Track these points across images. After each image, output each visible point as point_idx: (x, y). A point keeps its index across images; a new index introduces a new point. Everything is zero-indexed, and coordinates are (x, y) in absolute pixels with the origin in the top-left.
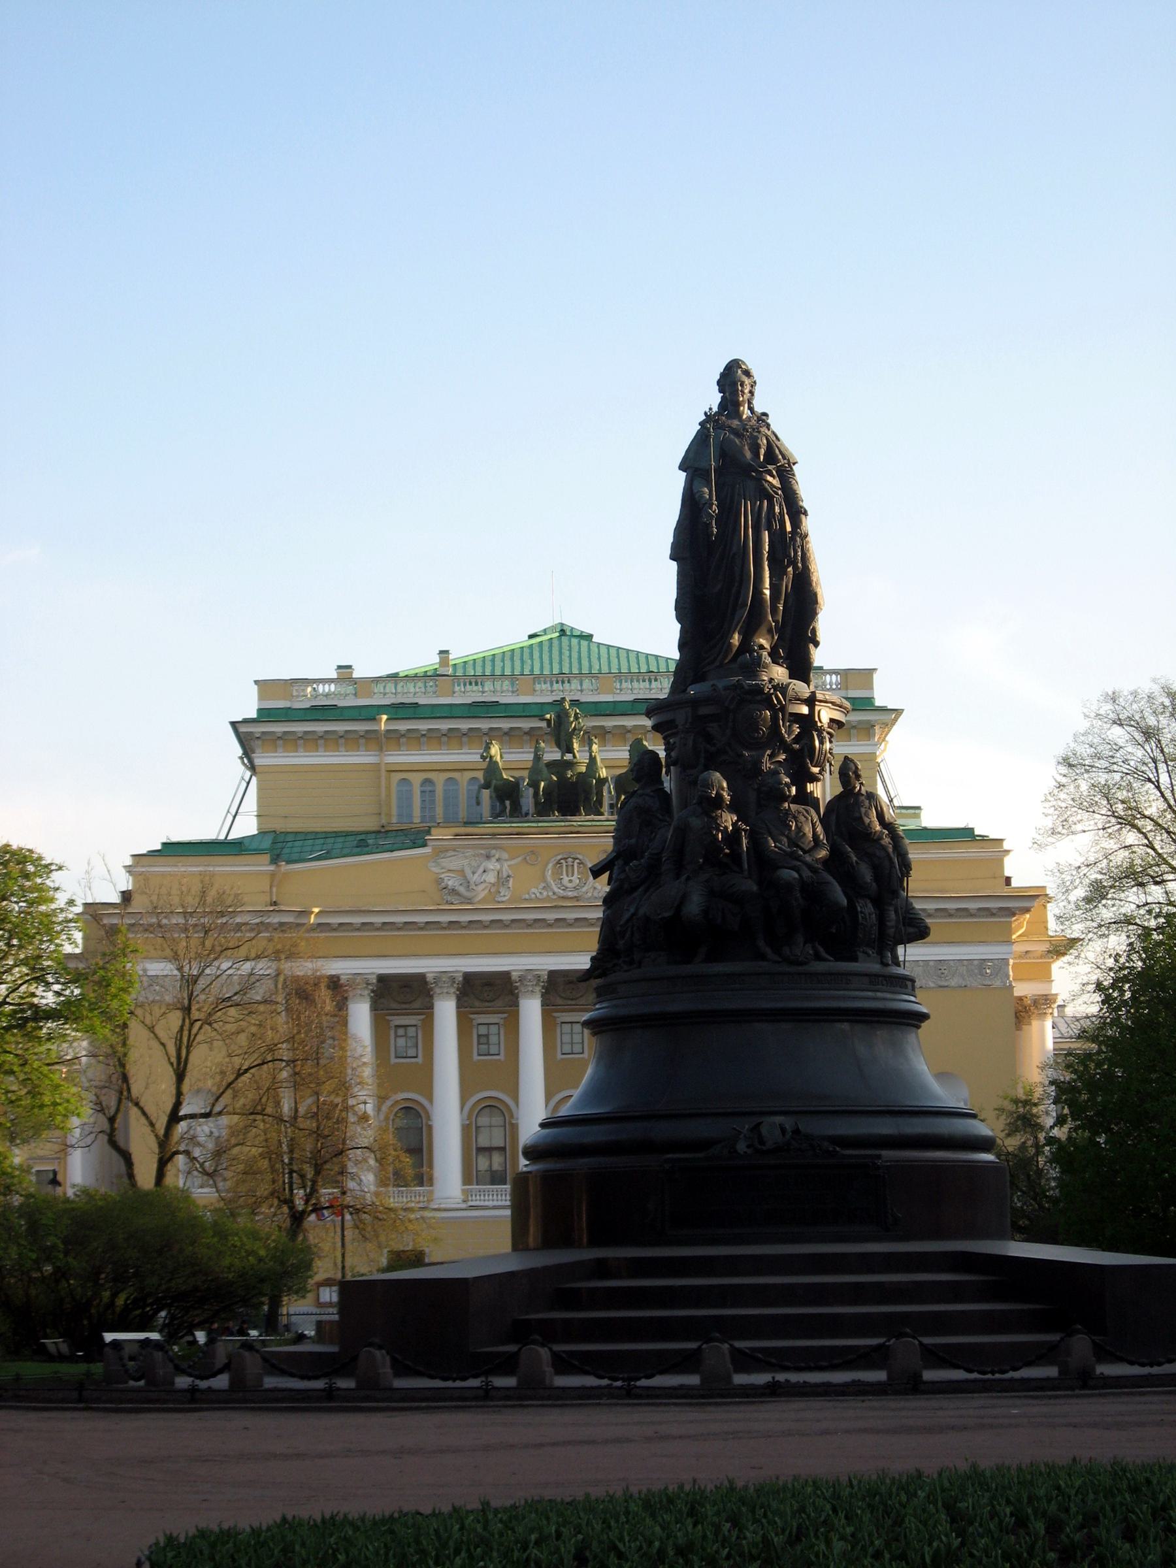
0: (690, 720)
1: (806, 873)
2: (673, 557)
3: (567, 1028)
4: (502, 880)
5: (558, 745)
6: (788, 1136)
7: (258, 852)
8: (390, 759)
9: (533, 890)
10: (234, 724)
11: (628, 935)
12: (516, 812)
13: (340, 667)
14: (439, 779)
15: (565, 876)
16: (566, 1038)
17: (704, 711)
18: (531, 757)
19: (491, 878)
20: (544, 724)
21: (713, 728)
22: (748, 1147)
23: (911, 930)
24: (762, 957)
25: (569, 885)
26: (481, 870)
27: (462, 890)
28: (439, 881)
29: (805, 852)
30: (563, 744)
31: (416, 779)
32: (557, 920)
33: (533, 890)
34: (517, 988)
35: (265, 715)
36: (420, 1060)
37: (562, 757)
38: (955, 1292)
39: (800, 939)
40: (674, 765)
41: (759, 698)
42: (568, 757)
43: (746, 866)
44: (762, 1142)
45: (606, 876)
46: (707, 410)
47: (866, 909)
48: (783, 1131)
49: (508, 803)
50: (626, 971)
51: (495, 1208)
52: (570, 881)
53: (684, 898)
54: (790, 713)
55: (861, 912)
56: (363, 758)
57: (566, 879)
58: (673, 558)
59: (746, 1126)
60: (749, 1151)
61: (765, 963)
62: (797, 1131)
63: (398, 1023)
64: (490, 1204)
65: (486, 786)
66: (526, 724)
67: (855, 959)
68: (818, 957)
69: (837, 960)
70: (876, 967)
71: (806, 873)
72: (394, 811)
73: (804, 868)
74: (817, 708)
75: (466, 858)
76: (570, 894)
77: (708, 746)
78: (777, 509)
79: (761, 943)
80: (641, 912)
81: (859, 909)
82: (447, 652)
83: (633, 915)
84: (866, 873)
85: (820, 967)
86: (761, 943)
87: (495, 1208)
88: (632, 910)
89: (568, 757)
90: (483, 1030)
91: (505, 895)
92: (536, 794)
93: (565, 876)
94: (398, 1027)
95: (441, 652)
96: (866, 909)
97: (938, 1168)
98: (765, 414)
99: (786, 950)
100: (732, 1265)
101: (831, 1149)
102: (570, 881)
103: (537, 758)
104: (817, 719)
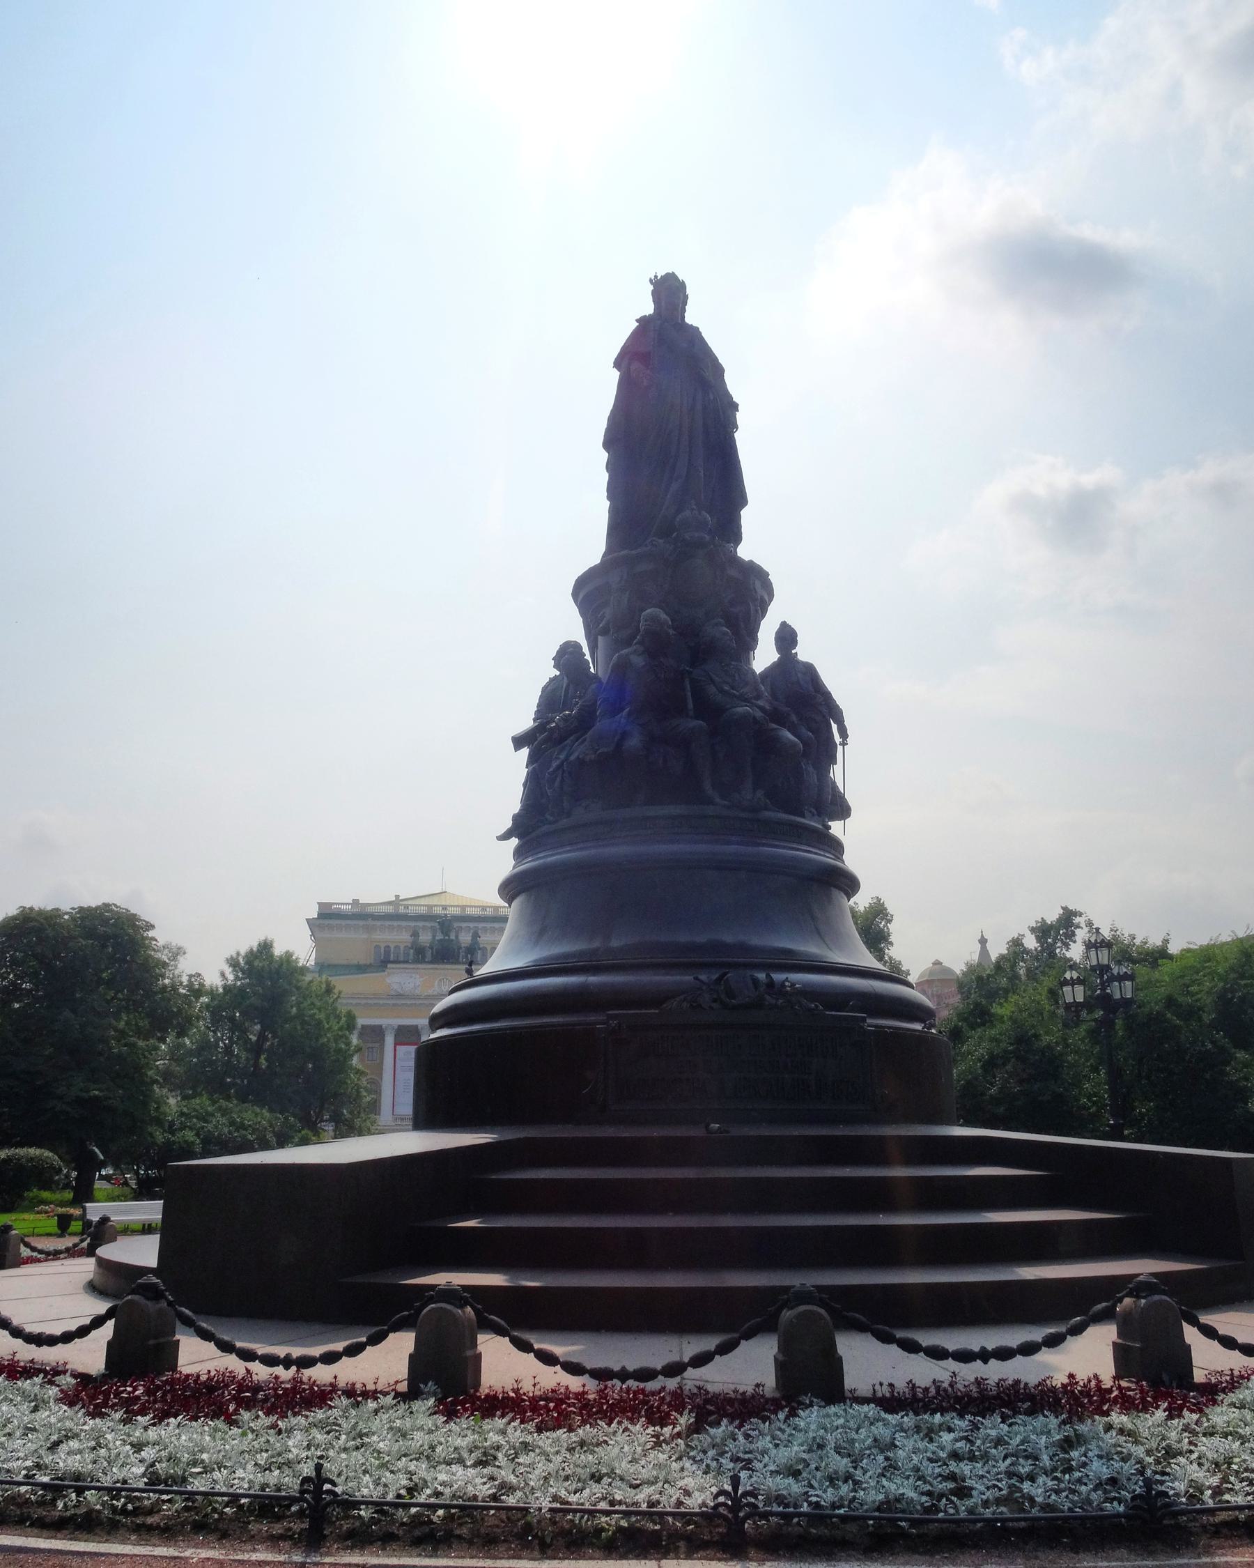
2: (608, 444)
5: (442, 933)
11: (557, 784)
12: (422, 961)
14: (392, 946)
18: (431, 937)
20: (436, 924)
35: (322, 915)
40: (605, 632)
42: (447, 938)
43: (690, 705)
45: (525, 752)
48: (756, 982)
50: (550, 823)
53: (624, 735)
57: (443, 988)
62: (771, 984)
65: (412, 948)
66: (428, 924)
68: (766, 809)
80: (572, 758)
83: (562, 764)
86: (708, 786)
88: (562, 757)
89: (447, 938)
92: (432, 953)
103: (434, 937)
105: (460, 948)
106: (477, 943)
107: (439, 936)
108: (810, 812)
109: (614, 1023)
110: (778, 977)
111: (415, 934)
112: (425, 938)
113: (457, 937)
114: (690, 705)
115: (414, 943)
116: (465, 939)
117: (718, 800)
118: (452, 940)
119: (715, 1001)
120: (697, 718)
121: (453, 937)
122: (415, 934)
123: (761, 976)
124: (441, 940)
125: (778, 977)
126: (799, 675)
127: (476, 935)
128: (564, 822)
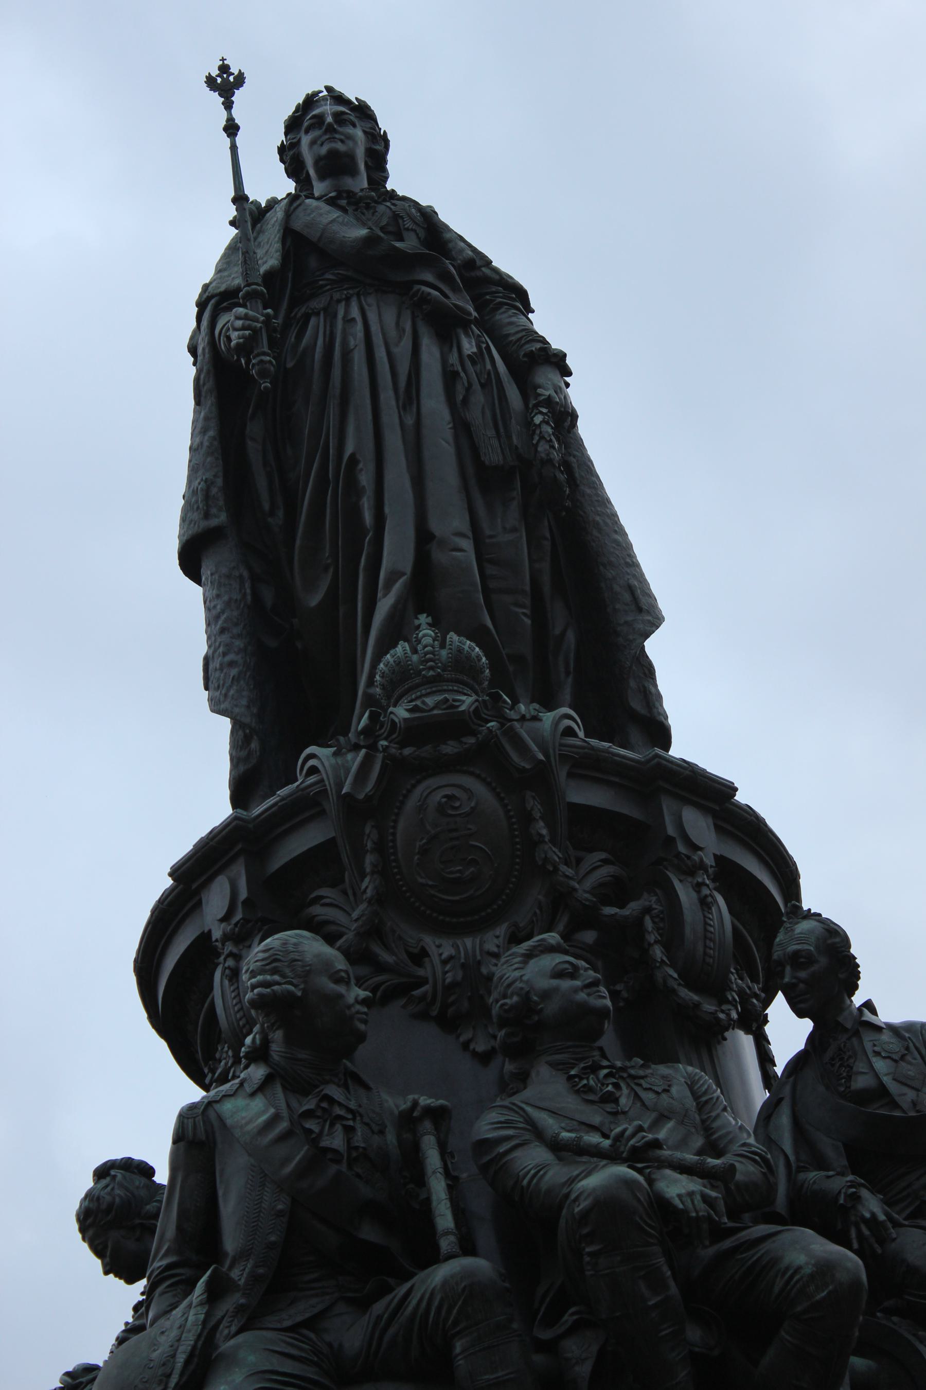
0: (243, 894)
41: (450, 748)
43: (445, 1219)
46: (215, 72)
54: (573, 807)
74: (668, 806)
114: (445, 1219)
120: (468, 1248)
126: (880, 1065)
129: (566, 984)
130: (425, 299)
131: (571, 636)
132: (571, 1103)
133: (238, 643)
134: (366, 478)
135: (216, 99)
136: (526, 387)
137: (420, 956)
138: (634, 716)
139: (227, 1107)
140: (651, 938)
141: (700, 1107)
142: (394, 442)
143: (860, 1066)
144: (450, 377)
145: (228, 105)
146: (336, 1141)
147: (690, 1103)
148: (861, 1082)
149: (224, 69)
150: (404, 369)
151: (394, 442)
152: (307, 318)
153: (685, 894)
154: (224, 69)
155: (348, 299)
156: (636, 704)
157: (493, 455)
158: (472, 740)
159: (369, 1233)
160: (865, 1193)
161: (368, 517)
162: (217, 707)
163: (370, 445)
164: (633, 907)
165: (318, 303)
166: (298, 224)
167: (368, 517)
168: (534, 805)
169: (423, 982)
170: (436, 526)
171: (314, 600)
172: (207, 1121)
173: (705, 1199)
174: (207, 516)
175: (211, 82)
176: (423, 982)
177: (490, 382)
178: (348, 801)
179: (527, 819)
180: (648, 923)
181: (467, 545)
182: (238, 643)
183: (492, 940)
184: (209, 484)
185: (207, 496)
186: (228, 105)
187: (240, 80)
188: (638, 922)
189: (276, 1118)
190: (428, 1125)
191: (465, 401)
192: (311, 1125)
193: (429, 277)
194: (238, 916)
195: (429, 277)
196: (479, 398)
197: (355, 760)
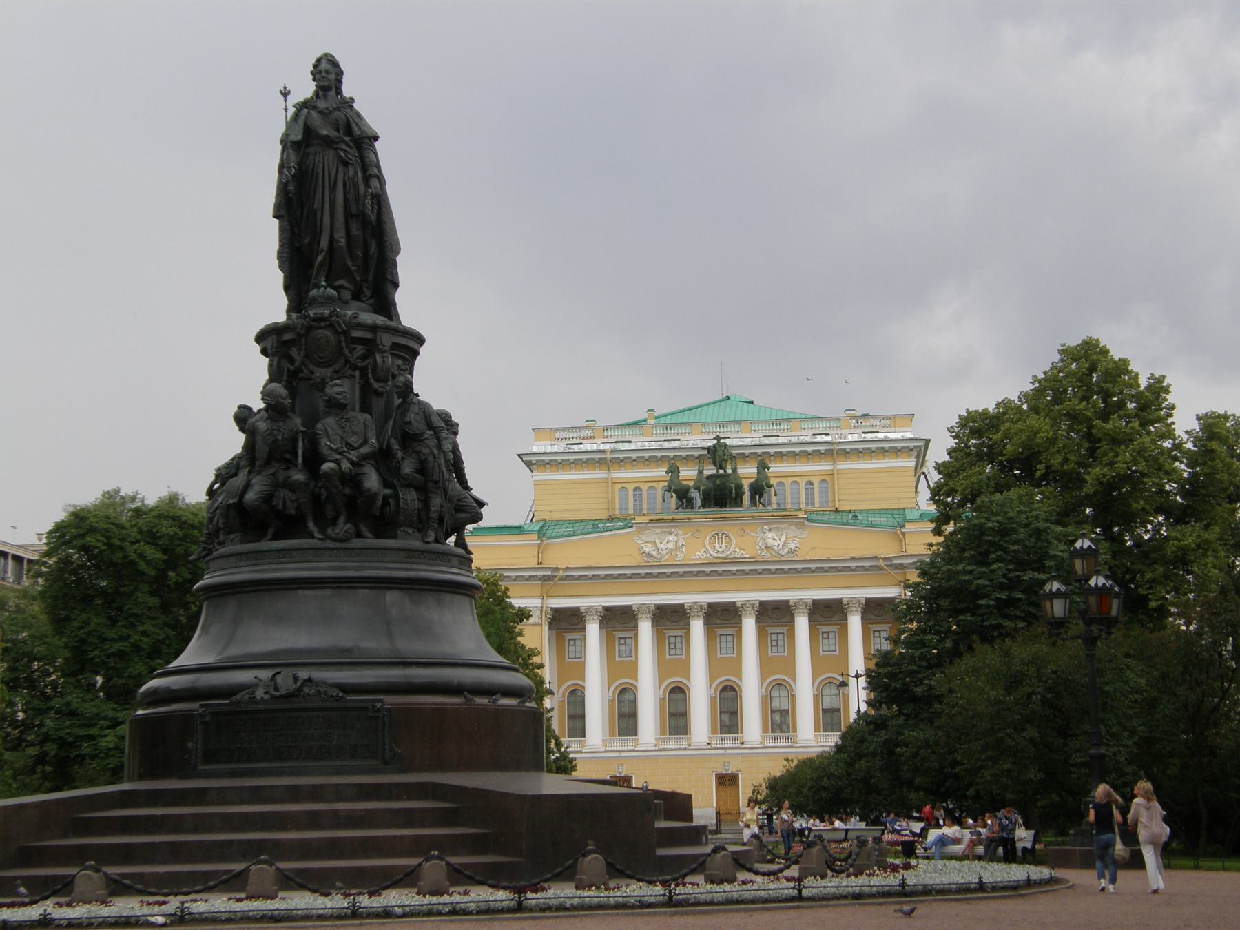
1: (346, 465)
3: (723, 638)
4: (678, 548)
6: (298, 684)
7: (532, 532)
8: (614, 476)
9: (697, 553)
10: (519, 455)
12: (690, 504)
13: (587, 421)
14: (645, 487)
15: (717, 544)
16: (724, 645)
17: (287, 337)
19: (671, 546)
21: (294, 352)
22: (266, 693)
23: (463, 515)
24: (313, 537)
25: (720, 550)
26: (666, 541)
27: (654, 553)
28: (640, 549)
29: (354, 448)
30: (718, 464)
31: (631, 487)
32: (712, 572)
33: (697, 553)
34: (688, 613)
36: (633, 658)
37: (718, 471)
38: (408, 818)
39: (342, 520)
41: (323, 324)
42: (721, 471)
44: (276, 689)
46: (282, 89)
47: (410, 498)
48: (296, 678)
49: (685, 501)
51: (680, 749)
52: (721, 547)
53: (247, 486)
55: (403, 498)
56: (599, 475)
58: (276, 217)
59: (264, 674)
60: (266, 697)
61: (310, 541)
63: (620, 636)
64: (673, 747)
67: (394, 537)
68: (359, 535)
69: (378, 536)
70: (416, 544)
71: (346, 465)
72: (617, 506)
73: (345, 461)
74: (379, 334)
75: (657, 534)
76: (720, 555)
77: (289, 366)
78: (351, 172)
79: (311, 525)
81: (401, 495)
82: (653, 410)
84: (408, 468)
85: (357, 543)
86: (311, 525)
87: (680, 749)
89: (721, 471)
90: (672, 640)
91: (680, 558)
93: (717, 544)
94: (620, 638)
95: (649, 410)
96: (410, 498)
97: (440, 711)
98: (352, 99)
99: (329, 531)
100: (256, 795)
101: (335, 694)
102: (721, 547)
103: (701, 472)
104: (378, 342)
105: (739, 487)
106: (767, 478)
107: (710, 470)
108: (406, 532)
109: (201, 711)
110: (318, 674)
111: (673, 471)
112: (688, 474)
113: (734, 470)
115: (670, 483)
116: (747, 472)
117: (316, 534)
118: (729, 475)
119: (266, 693)
121: (729, 471)
122: (673, 471)
123: (303, 674)
124: (709, 477)
125: (318, 674)
126: (412, 415)
127: (763, 467)
128: (222, 551)
129: (339, 397)
130: (340, 156)
131: (375, 256)
132: (335, 426)
133: (286, 250)
134: (319, 216)
135: (282, 97)
136: (368, 185)
137: (312, 373)
138: (388, 280)
139: (258, 423)
140: (370, 371)
141: (365, 428)
142: (327, 206)
143: (408, 415)
144: (345, 185)
145: (285, 101)
146: (280, 437)
147: (363, 428)
148: (407, 419)
149: (285, 88)
150: (333, 179)
151: (327, 206)
152: (309, 154)
153: (378, 359)
154: (285, 88)
155: (320, 152)
156: (389, 277)
157: (354, 210)
158: (327, 323)
159: (287, 456)
160: (399, 452)
161: (318, 229)
162: (281, 267)
163: (320, 206)
164: (367, 362)
165: (312, 150)
166: (308, 123)
167: (318, 229)
168: (343, 338)
169: (312, 379)
170: (336, 236)
171: (306, 241)
172: (254, 427)
173: (350, 470)
174: (280, 211)
175: (281, 92)
176: (312, 379)
177: (356, 186)
178: (299, 335)
179: (340, 342)
180: (369, 367)
181: (343, 241)
182: (286, 250)
183: (328, 372)
184: (281, 202)
185: (279, 205)
186: (285, 101)
187: (289, 93)
188: (365, 368)
189: (267, 430)
190: (300, 434)
191: (349, 193)
192: (275, 432)
193: (343, 146)
194: (274, 350)
195: (343, 146)
196: (352, 191)
197: (301, 321)
